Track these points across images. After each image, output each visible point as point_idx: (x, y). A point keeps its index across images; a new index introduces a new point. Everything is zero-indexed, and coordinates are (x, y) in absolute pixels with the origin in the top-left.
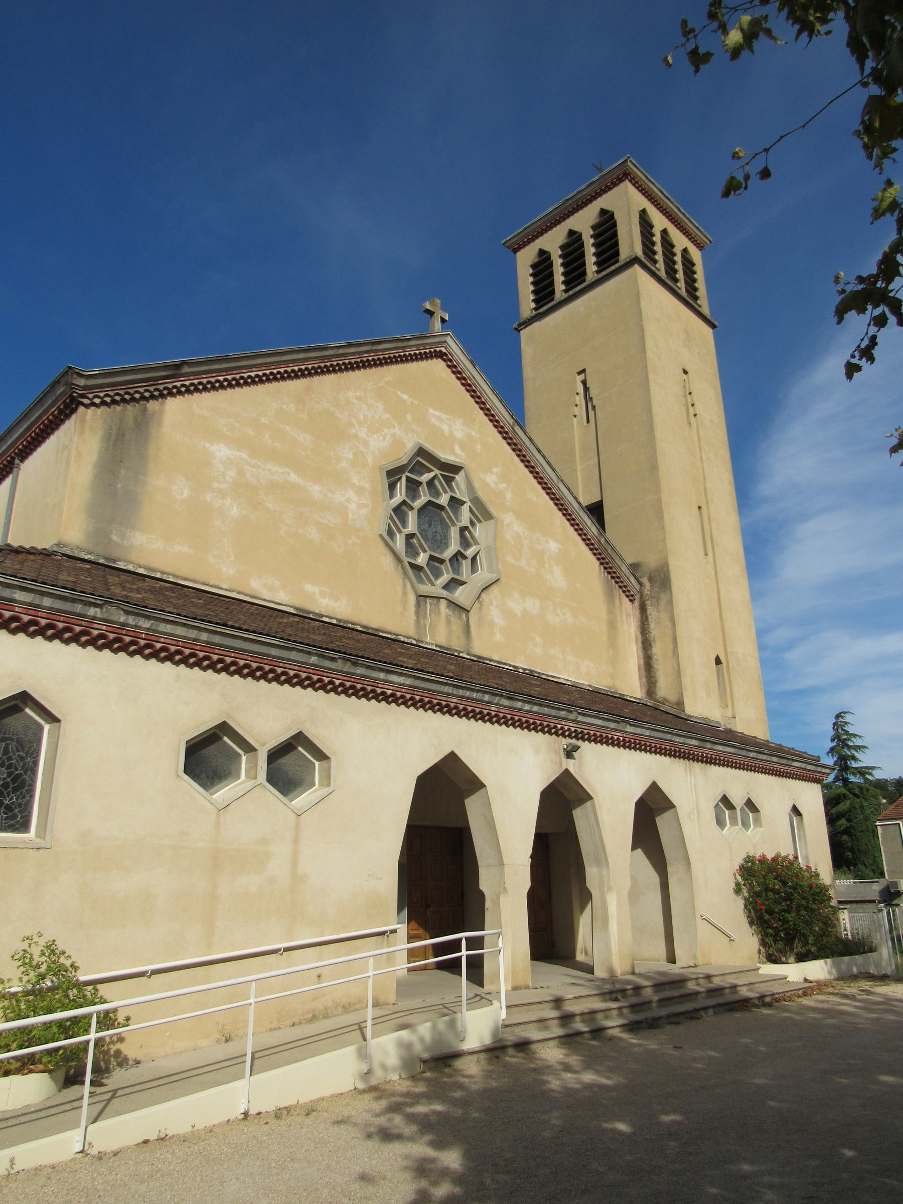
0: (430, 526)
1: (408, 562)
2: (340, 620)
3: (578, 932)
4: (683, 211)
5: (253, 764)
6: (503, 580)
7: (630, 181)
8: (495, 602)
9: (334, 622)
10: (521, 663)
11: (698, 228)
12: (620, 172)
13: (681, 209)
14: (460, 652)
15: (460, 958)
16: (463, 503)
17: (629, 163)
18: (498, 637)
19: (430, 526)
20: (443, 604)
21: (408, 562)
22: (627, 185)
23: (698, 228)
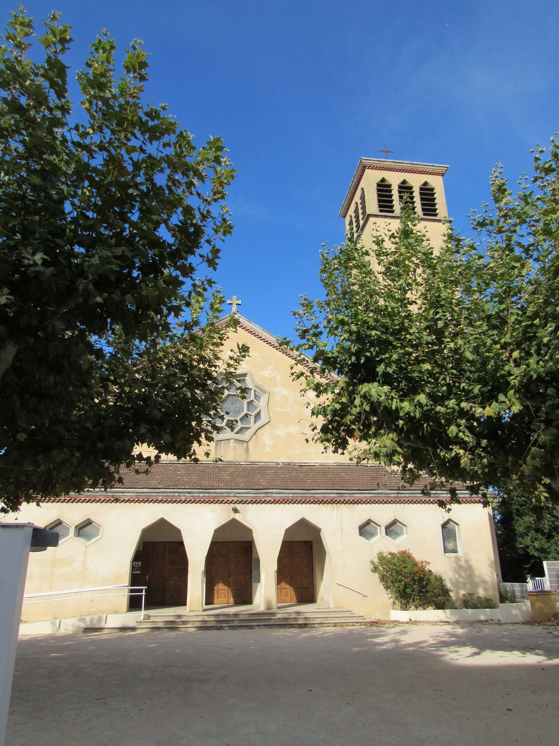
0: (232, 405)
1: (255, 422)
2: (171, 461)
3: (319, 589)
4: (416, 163)
5: (381, 531)
6: (272, 421)
7: (369, 168)
8: (266, 433)
9: (168, 462)
10: (283, 459)
11: (433, 166)
12: (361, 167)
13: (414, 163)
14: (240, 462)
15: (142, 595)
16: (251, 389)
17: (363, 161)
18: (268, 450)
19: (232, 405)
20: (232, 442)
21: (255, 422)
22: (367, 171)
23: (433, 166)
